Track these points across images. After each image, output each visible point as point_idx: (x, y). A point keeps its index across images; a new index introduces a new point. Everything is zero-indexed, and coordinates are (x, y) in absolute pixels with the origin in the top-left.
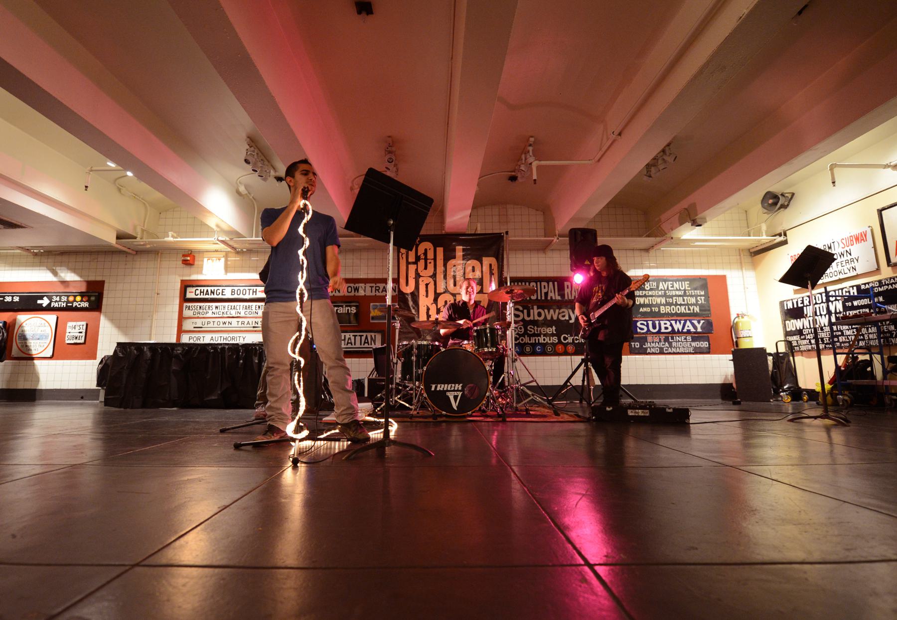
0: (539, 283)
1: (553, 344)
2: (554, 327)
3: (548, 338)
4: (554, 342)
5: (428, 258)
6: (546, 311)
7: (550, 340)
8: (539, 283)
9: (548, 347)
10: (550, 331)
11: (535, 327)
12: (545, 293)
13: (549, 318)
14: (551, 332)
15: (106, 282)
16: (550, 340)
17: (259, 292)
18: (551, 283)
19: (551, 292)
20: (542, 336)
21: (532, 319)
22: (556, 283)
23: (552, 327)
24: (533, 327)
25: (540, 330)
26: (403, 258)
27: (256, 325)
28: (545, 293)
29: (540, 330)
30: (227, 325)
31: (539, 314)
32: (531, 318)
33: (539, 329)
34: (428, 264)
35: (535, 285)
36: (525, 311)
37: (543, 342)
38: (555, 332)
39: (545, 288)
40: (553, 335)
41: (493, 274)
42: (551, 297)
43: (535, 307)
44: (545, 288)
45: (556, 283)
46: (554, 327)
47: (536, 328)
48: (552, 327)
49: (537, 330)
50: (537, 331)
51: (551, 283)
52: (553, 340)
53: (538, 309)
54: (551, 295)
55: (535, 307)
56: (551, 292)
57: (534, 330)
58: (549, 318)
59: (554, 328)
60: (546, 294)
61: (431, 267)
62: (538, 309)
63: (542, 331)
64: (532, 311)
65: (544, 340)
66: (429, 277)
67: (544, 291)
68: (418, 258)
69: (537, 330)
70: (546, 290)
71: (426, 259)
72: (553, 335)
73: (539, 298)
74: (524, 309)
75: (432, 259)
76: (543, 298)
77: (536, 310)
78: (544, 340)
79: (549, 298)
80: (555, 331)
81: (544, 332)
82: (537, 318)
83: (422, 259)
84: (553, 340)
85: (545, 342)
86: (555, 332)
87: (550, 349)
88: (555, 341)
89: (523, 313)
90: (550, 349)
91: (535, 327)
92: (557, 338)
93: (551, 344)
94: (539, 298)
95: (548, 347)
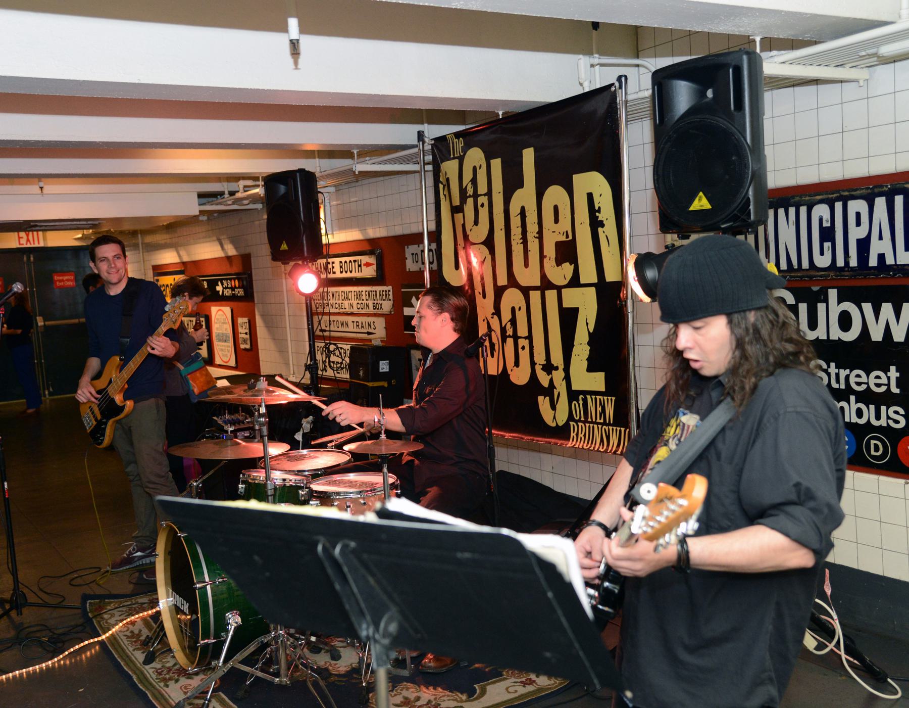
0: (838, 206)
1: (887, 431)
2: (893, 368)
3: (872, 407)
4: (891, 423)
5: (479, 193)
6: (867, 307)
7: (878, 417)
8: (838, 206)
9: (873, 442)
10: (878, 385)
11: (833, 365)
12: (859, 241)
13: (877, 335)
14: (883, 389)
15: (252, 255)
16: (878, 417)
17: (374, 264)
18: (880, 203)
19: (881, 238)
20: (852, 398)
21: (823, 337)
22: (899, 200)
23: (886, 370)
24: (825, 366)
25: (847, 377)
26: (445, 195)
27: (370, 331)
28: (859, 241)
29: (847, 377)
30: (351, 329)
31: (845, 321)
32: (820, 333)
33: (843, 373)
34: (480, 208)
35: (826, 215)
36: (803, 308)
37: (855, 419)
38: (895, 390)
39: (858, 223)
40: (887, 399)
41: (602, 224)
42: (881, 257)
43: (833, 294)
44: (858, 223)
45: (899, 200)
46: (893, 368)
47: (833, 369)
48: (886, 370)
49: (837, 375)
50: (838, 381)
51: (880, 203)
52: (888, 418)
53: (840, 301)
54: (877, 247)
55: (833, 294)
56: (881, 238)
57: (829, 375)
58: (877, 335)
59: (893, 373)
60: (864, 245)
61: (484, 213)
62: (840, 301)
63: (853, 380)
64: (821, 307)
65: (859, 413)
66: (481, 243)
67: (856, 233)
68: (463, 196)
69: (837, 375)
70: (862, 232)
71: (476, 196)
72: (887, 399)
73: (840, 263)
74: (798, 300)
75: (485, 195)
76: (853, 263)
77: (834, 306)
78: (859, 413)
79: (873, 262)
80: (897, 387)
81: (859, 384)
82: (836, 333)
83: (470, 196)
84: (888, 418)
85: (862, 421)
86: (895, 390)
87: (877, 448)
88: (897, 422)
89: (797, 315)
90: (877, 448)
91: (833, 365)
92: (902, 411)
93: (880, 429)
94: (840, 263)
95: (873, 442)
